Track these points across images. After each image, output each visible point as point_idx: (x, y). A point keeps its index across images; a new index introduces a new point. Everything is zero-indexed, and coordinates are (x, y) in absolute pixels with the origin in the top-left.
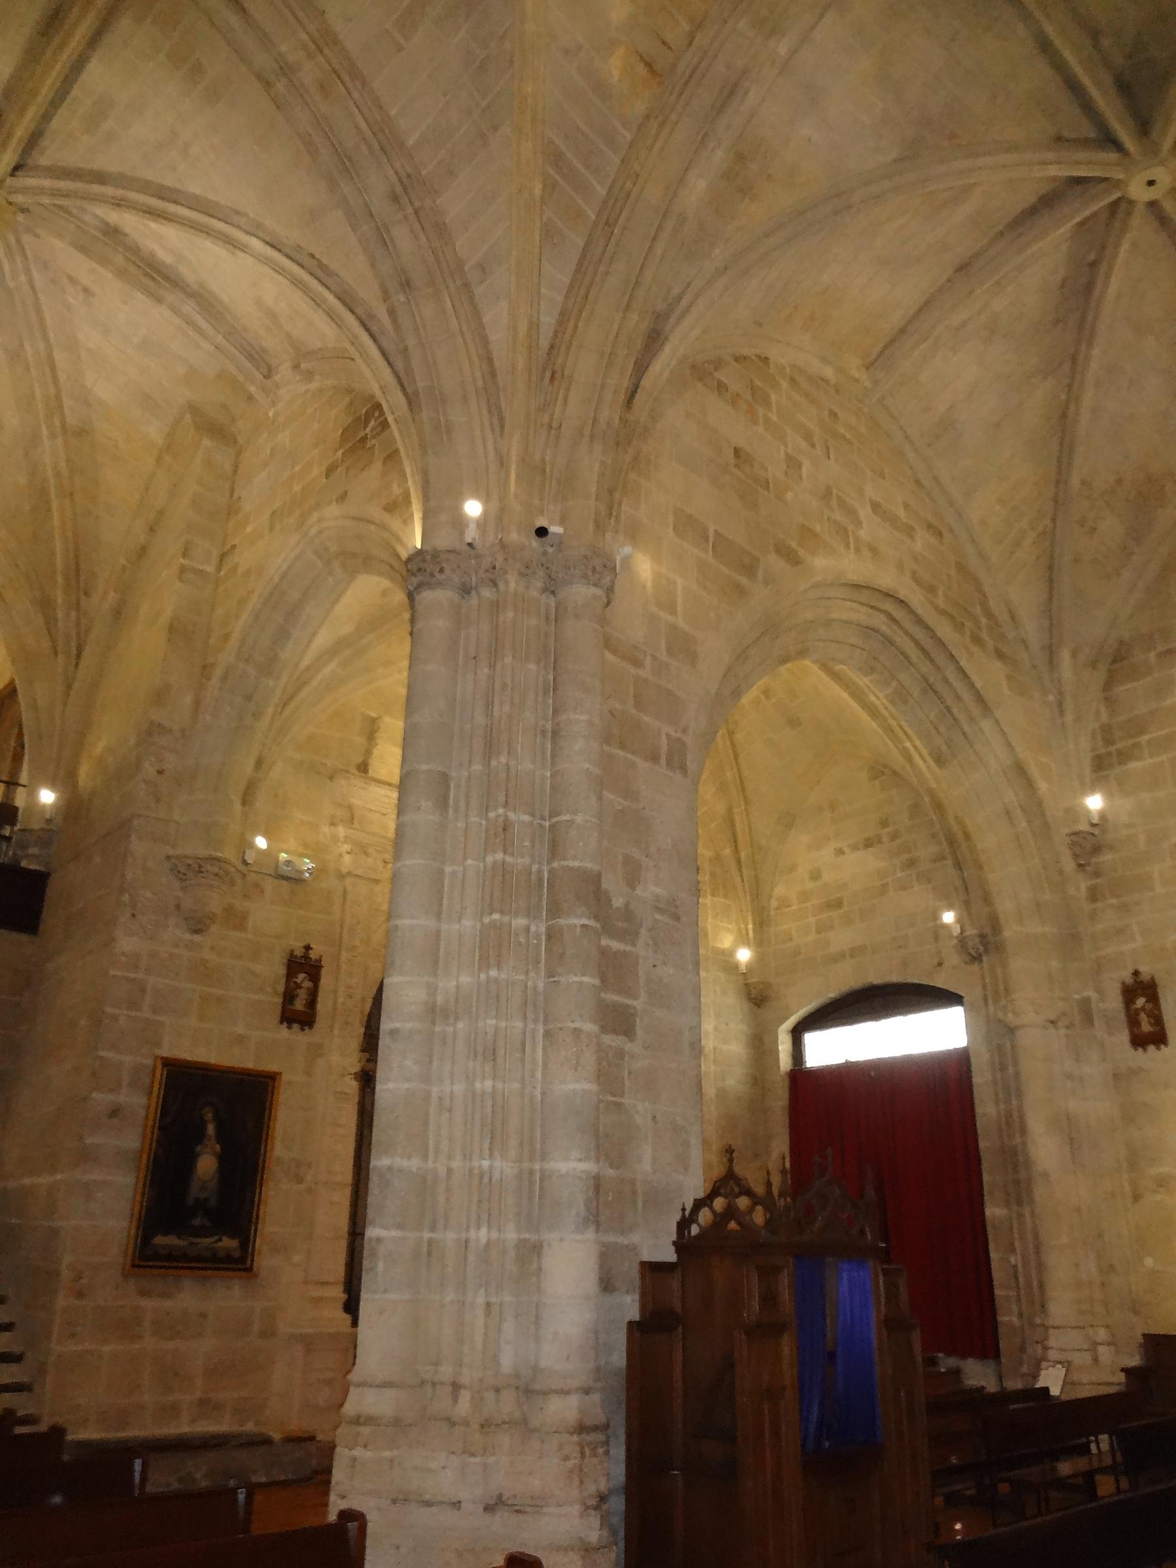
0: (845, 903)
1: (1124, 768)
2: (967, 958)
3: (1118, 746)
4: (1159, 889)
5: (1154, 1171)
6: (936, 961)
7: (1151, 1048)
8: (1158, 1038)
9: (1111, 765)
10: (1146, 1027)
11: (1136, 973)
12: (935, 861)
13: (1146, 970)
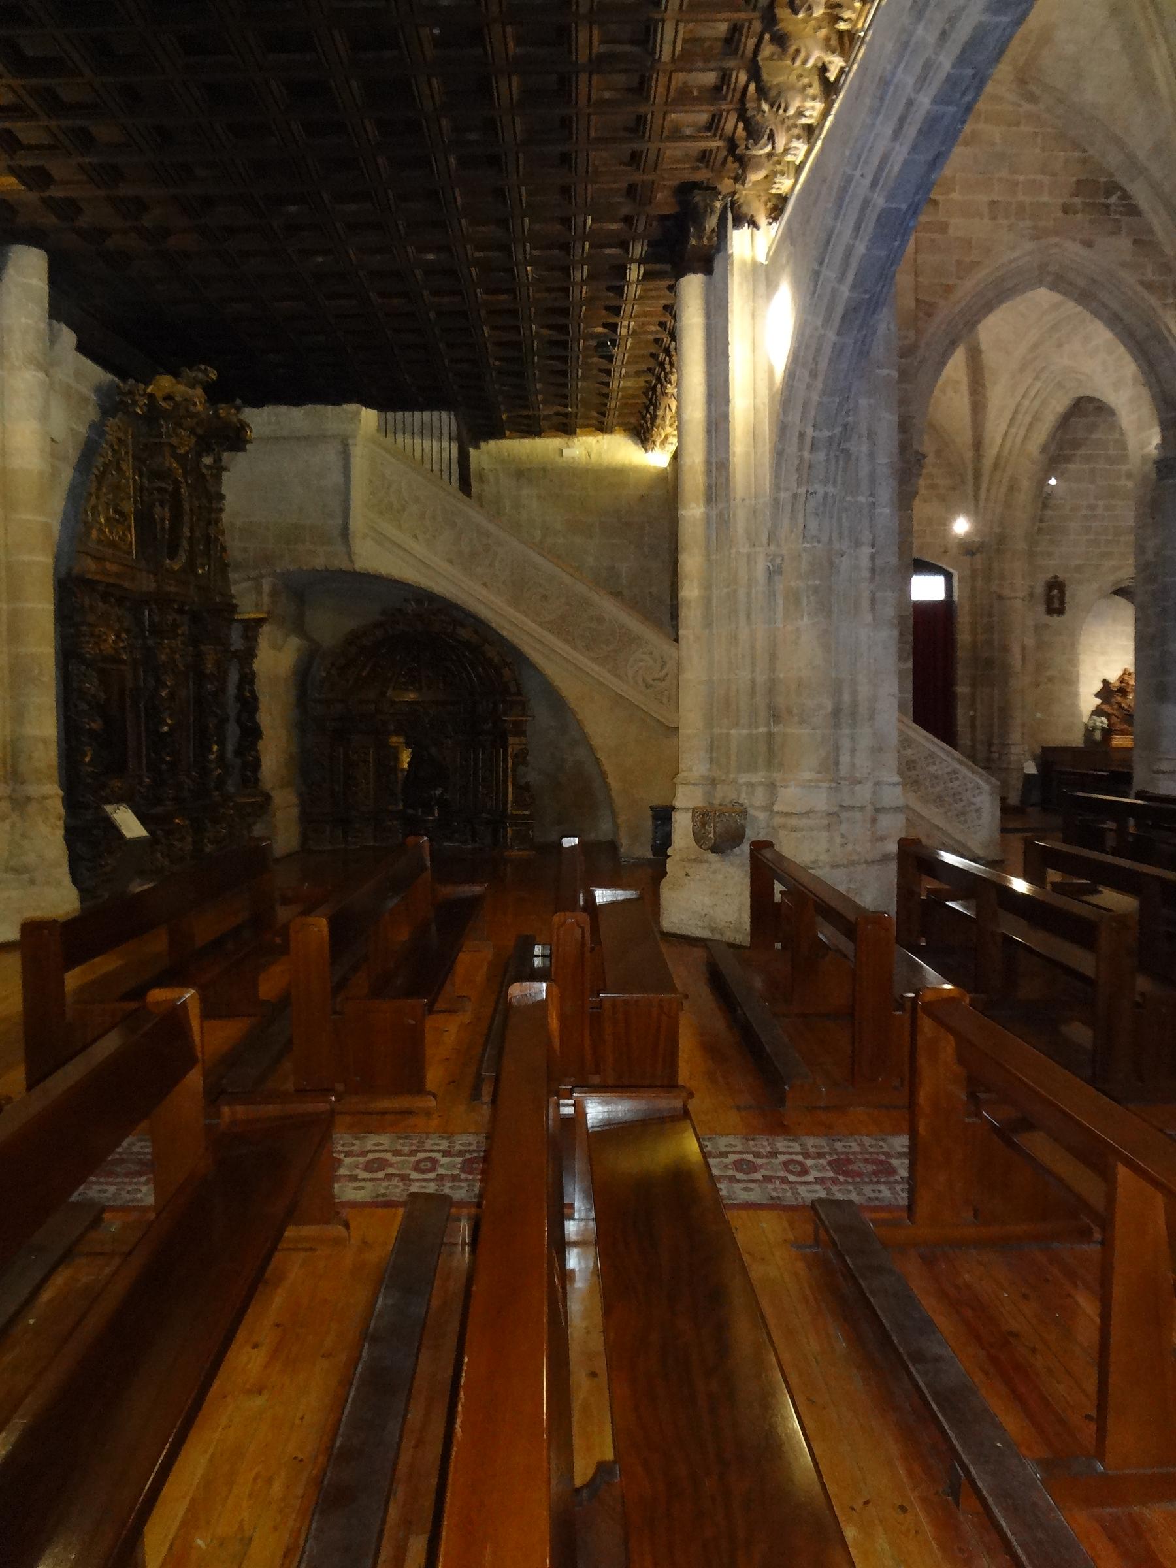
8: (1060, 611)
10: (1056, 605)
11: (1056, 577)
13: (1061, 576)
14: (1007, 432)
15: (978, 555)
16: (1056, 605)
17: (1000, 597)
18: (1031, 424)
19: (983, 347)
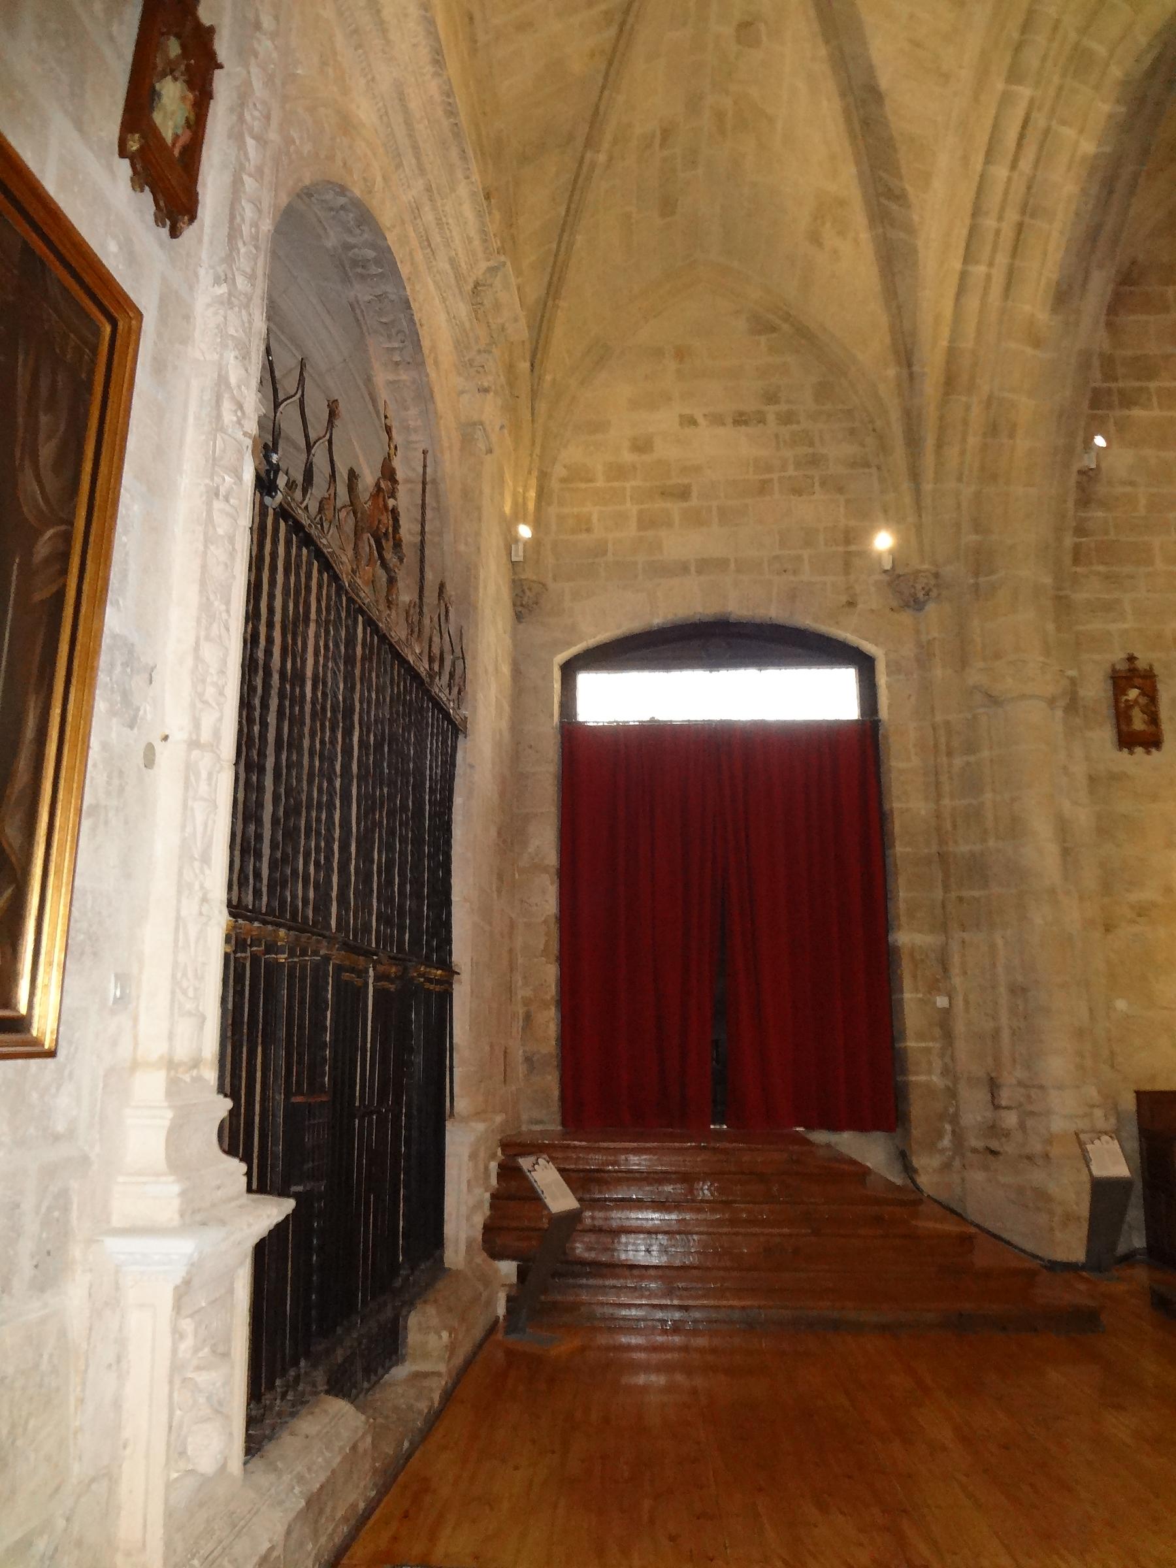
0: (694, 494)
1: (1126, 412)
2: (895, 604)
3: (1121, 384)
4: (1160, 565)
5: (1135, 897)
6: (844, 599)
7: (1139, 750)
8: (1152, 741)
9: (1110, 407)
10: (1139, 723)
11: (1131, 659)
12: (853, 465)
14: (964, 275)
15: (931, 607)
16: (1139, 723)
17: (993, 700)
18: (1020, 227)
19: (884, 83)
